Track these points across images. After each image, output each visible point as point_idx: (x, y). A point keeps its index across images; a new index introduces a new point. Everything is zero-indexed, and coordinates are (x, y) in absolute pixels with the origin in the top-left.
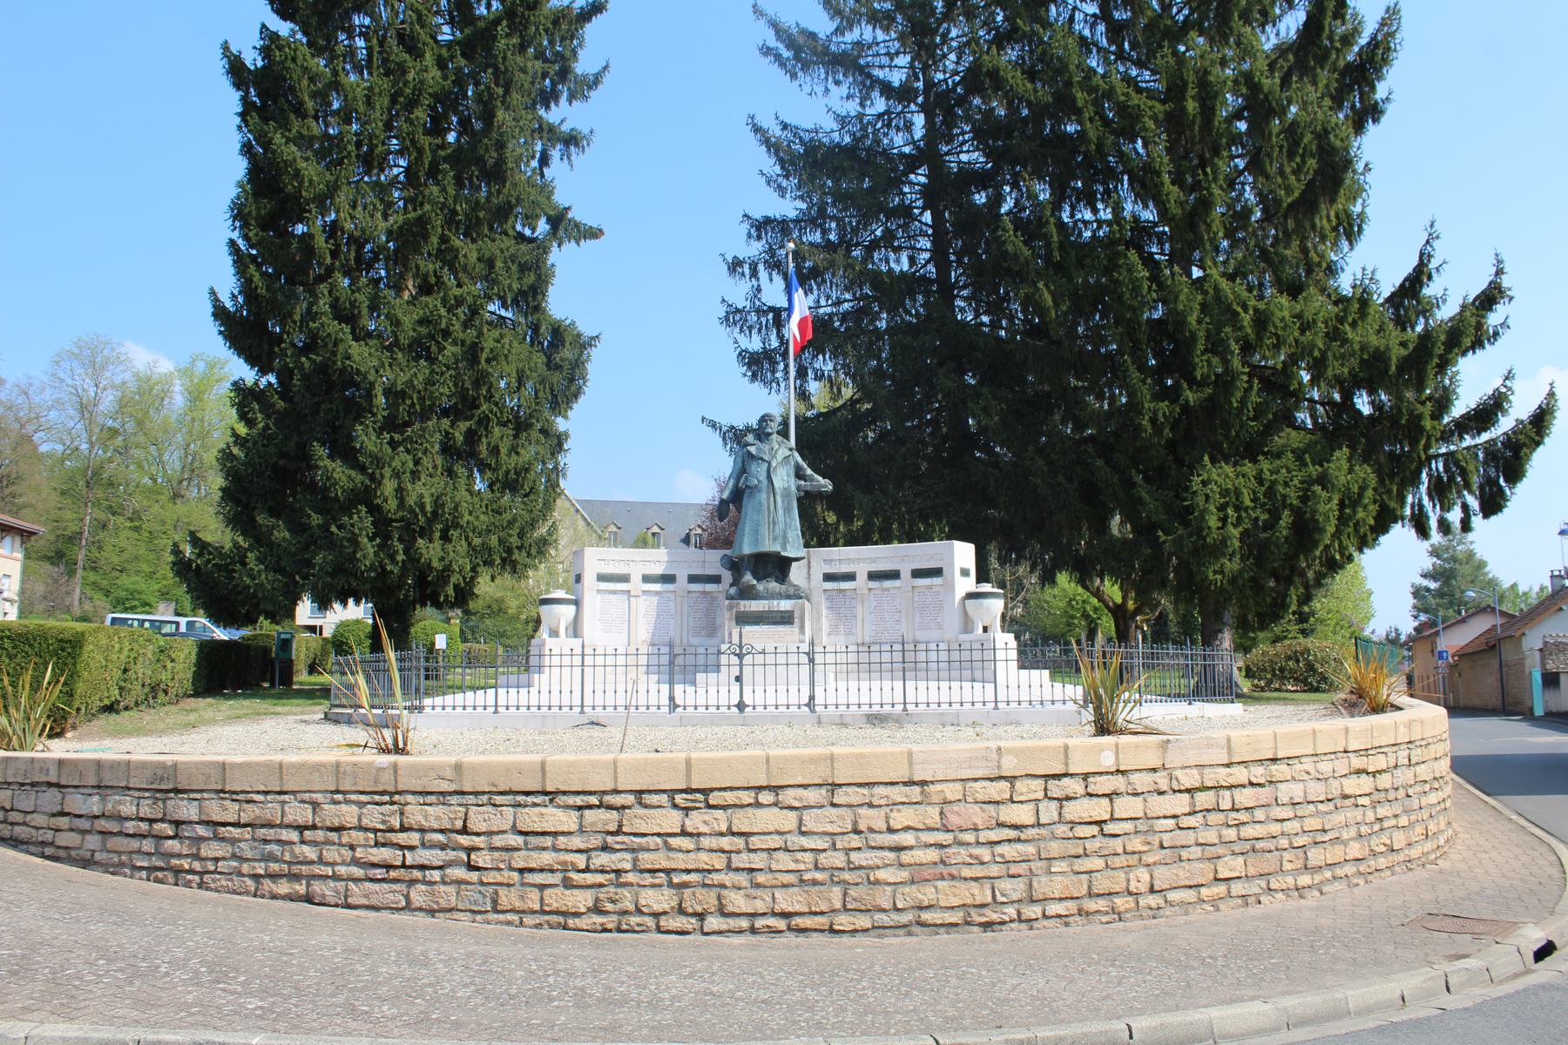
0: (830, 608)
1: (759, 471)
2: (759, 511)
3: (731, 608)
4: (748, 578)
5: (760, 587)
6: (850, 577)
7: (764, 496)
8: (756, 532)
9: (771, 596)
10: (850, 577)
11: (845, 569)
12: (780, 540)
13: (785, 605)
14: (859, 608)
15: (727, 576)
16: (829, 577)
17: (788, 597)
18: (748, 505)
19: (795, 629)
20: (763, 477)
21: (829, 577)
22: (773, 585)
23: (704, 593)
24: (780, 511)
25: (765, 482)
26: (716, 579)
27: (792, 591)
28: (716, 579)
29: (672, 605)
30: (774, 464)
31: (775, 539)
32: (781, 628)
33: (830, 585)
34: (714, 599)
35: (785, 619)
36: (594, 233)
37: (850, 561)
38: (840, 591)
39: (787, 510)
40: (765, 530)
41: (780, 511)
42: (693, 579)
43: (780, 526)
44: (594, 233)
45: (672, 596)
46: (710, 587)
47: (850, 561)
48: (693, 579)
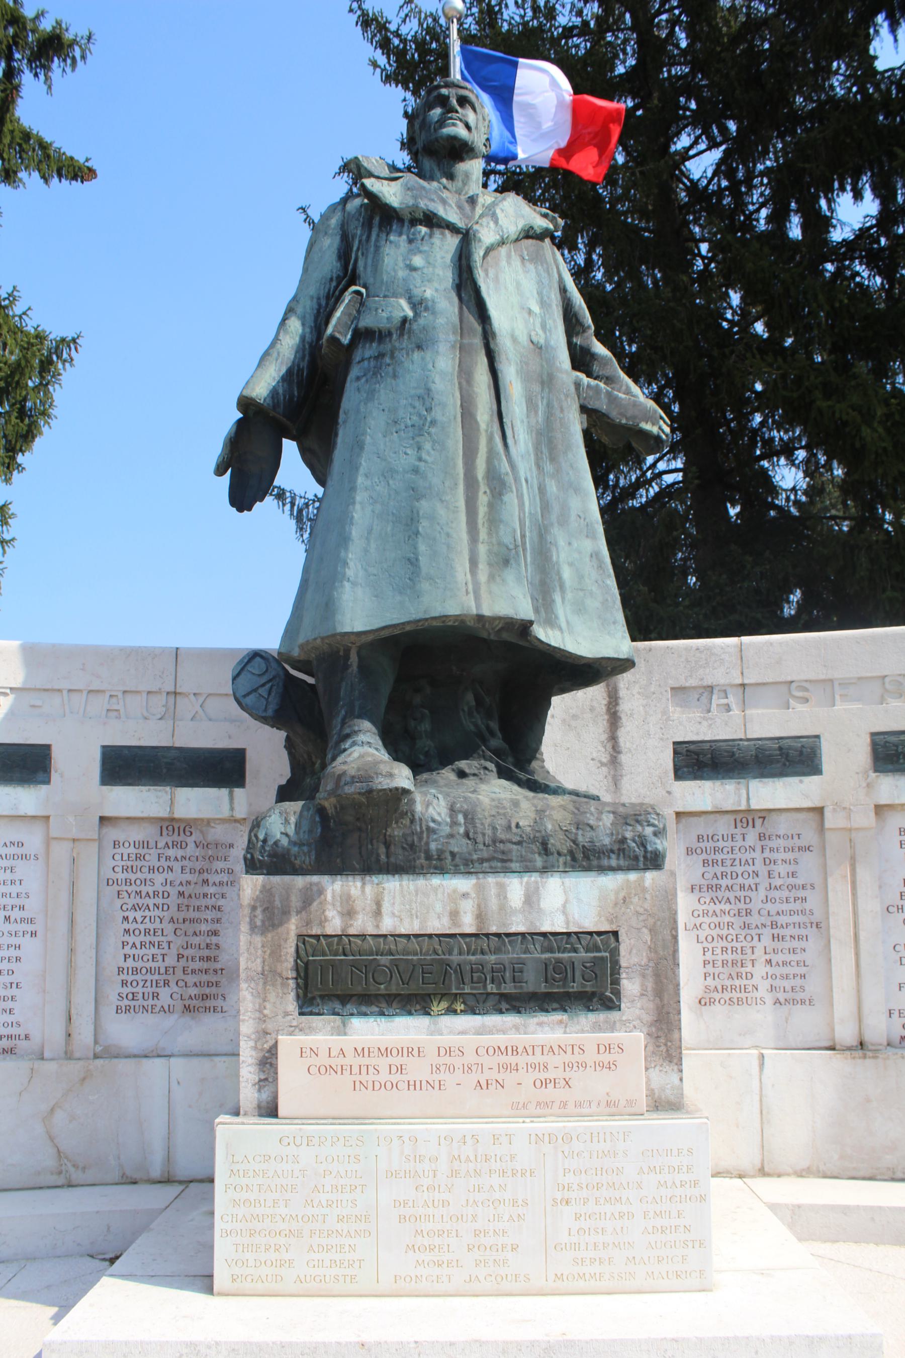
0: (708, 888)
1: (419, 270)
2: (421, 429)
3: (270, 915)
4: (364, 753)
5: (434, 802)
6: (795, 757)
7: (442, 362)
8: (408, 524)
9: (491, 853)
10: (795, 757)
11: (766, 723)
12: (526, 566)
13: (567, 902)
14: (839, 891)
15: (268, 752)
16: (697, 761)
17: (586, 858)
18: (369, 414)
19: (625, 1034)
20: (438, 287)
21: (697, 761)
22: (493, 793)
23: (172, 826)
24: (522, 440)
25: (446, 306)
26: (223, 769)
27: (604, 828)
28: (223, 769)
29: (31, 875)
30: (487, 235)
31: (504, 560)
32: (546, 1031)
33: (703, 794)
34: (214, 850)
35: (571, 978)
36: (79, 172)
37: (789, 691)
38: (748, 817)
39: (547, 442)
40: (449, 513)
41: (522, 440)
42: (123, 766)
43: (519, 507)
44: (79, 172)
45: (34, 840)
46: (195, 802)
47: (789, 691)
48: (123, 766)
